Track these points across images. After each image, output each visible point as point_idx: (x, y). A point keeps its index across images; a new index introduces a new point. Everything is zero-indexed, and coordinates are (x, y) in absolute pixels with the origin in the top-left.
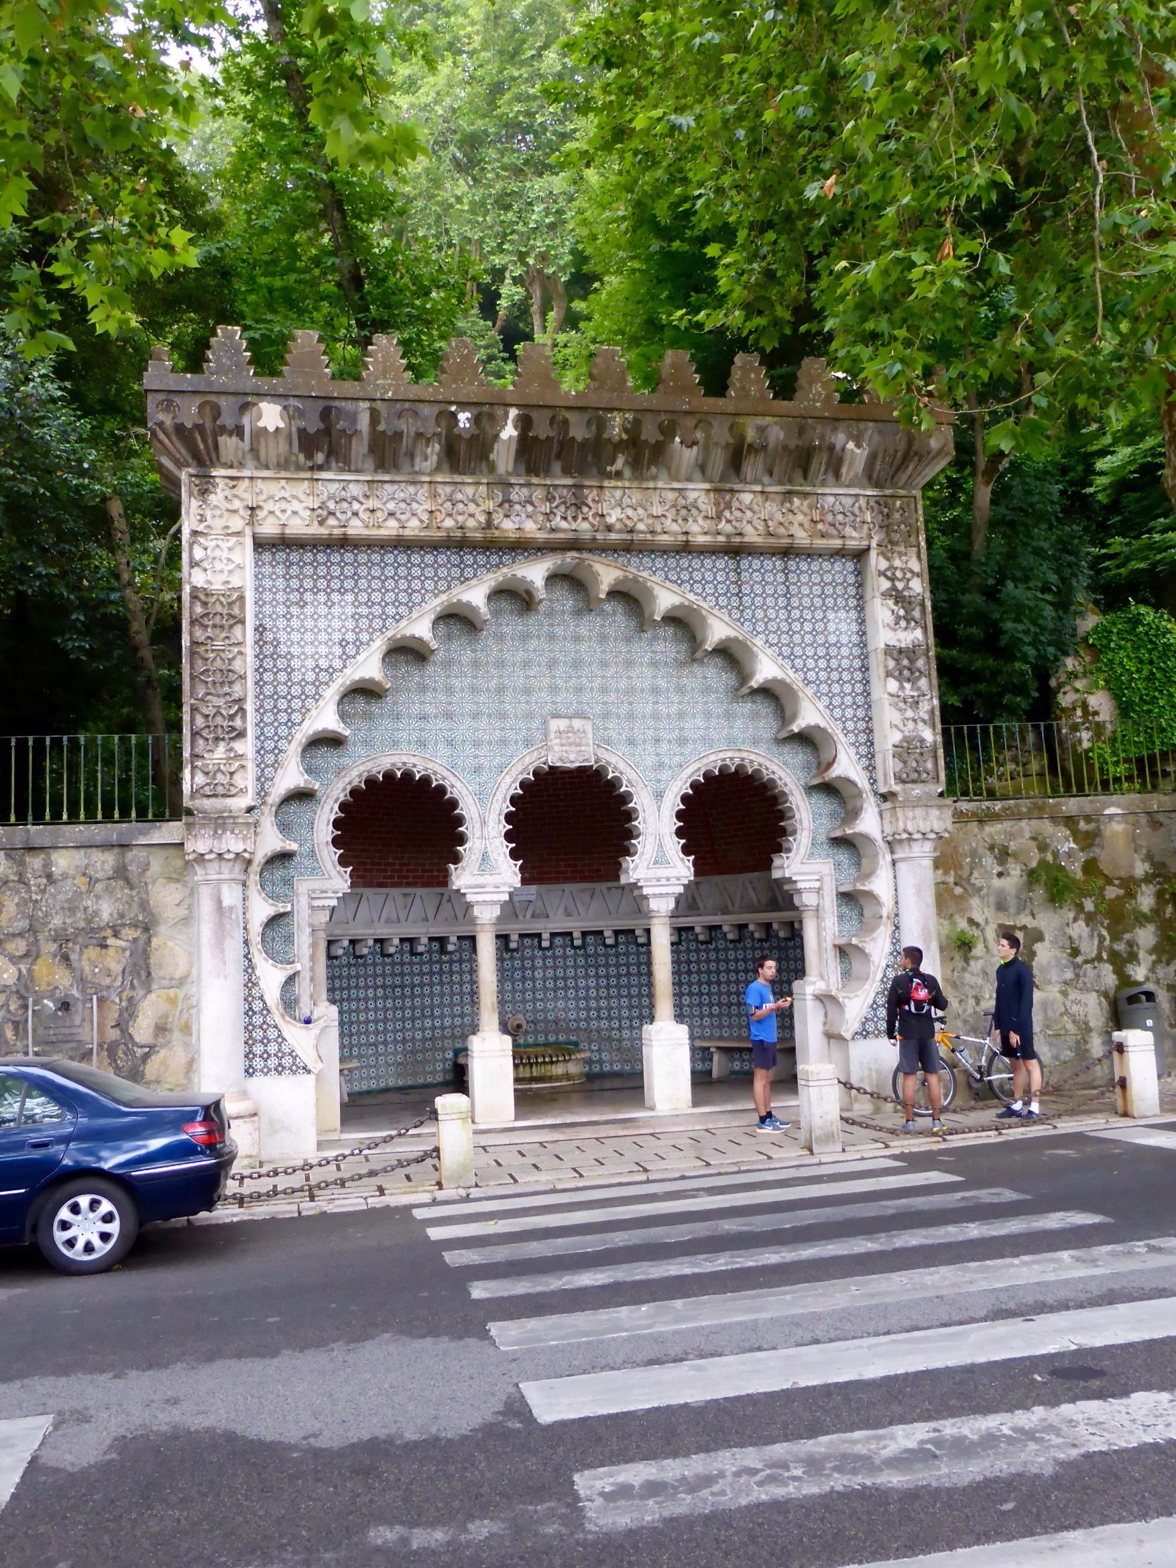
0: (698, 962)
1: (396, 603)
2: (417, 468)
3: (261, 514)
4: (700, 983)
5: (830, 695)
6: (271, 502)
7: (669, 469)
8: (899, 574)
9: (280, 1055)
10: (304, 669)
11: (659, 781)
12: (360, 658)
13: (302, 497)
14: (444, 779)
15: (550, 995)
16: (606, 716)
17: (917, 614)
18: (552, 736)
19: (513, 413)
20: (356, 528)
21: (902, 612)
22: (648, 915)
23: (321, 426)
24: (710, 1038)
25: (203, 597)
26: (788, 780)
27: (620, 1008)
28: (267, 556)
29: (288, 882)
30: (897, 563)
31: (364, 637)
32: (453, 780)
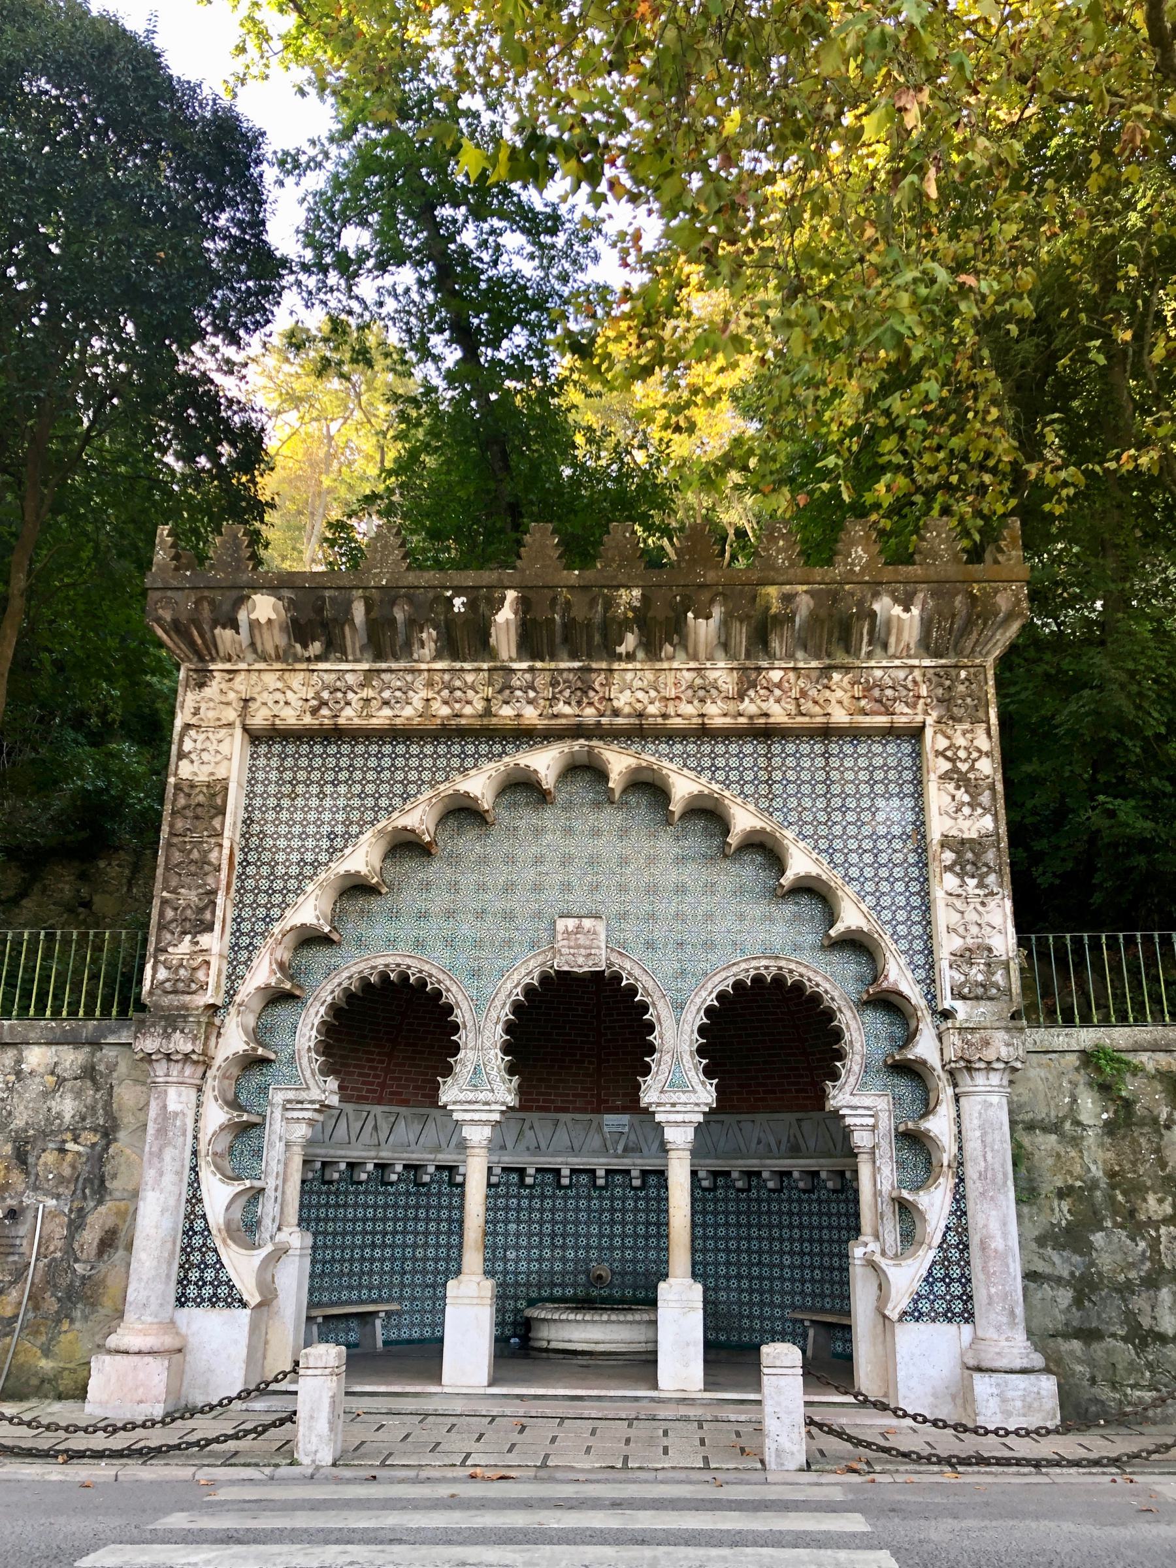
0: (800, 1214)
1: (391, 795)
2: (416, 656)
3: (253, 706)
4: (801, 1240)
5: (878, 895)
6: (265, 694)
7: (686, 648)
8: (962, 754)
9: (217, 1283)
10: (287, 861)
11: (679, 990)
12: (347, 851)
13: (295, 685)
14: (439, 982)
15: (641, 1242)
16: (623, 916)
17: (985, 798)
18: (559, 937)
19: (511, 595)
20: (349, 716)
21: (966, 798)
22: (663, 1148)
23: (312, 615)
24: (812, 1309)
25: (186, 790)
26: (836, 994)
27: (716, 1264)
28: (263, 749)
29: (263, 1090)
30: (961, 741)
31: (354, 829)
32: (448, 983)
